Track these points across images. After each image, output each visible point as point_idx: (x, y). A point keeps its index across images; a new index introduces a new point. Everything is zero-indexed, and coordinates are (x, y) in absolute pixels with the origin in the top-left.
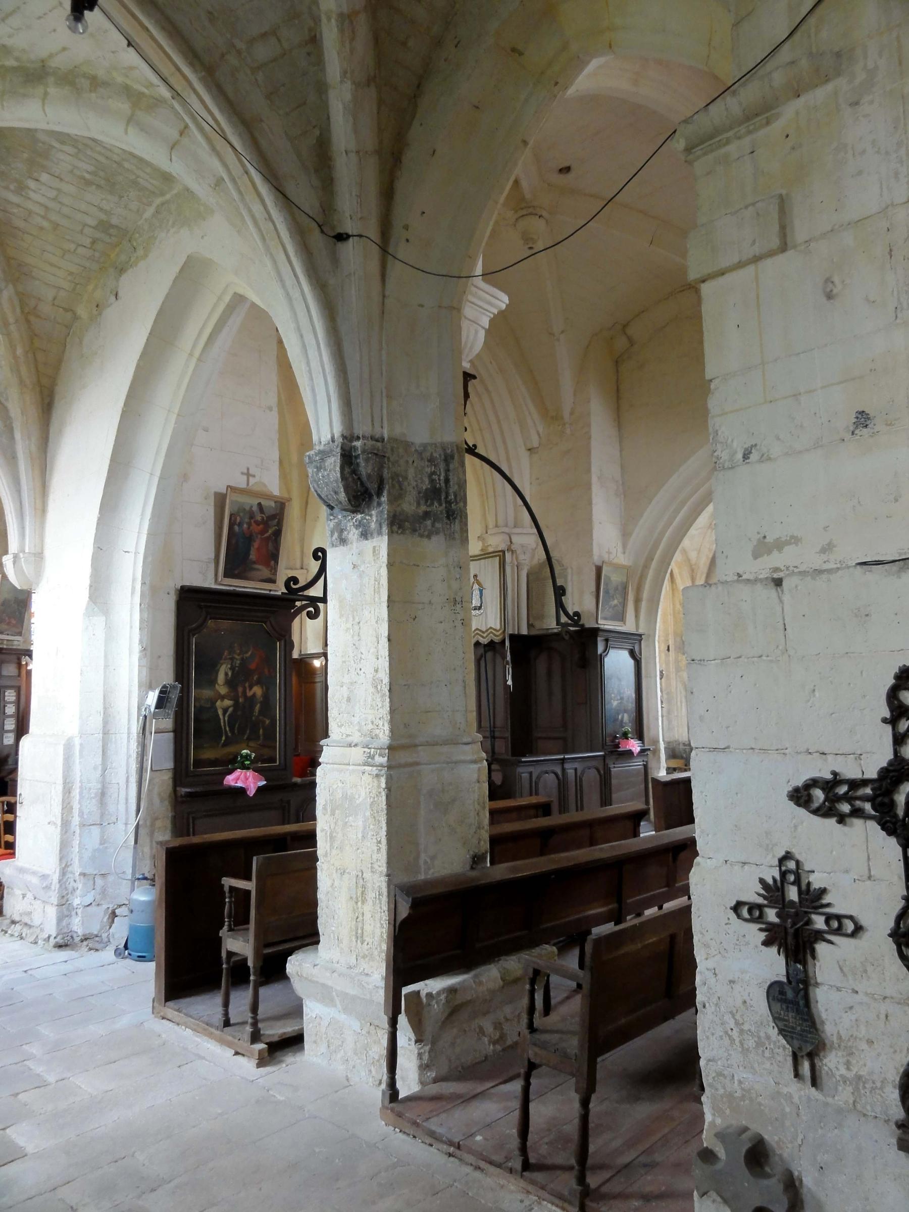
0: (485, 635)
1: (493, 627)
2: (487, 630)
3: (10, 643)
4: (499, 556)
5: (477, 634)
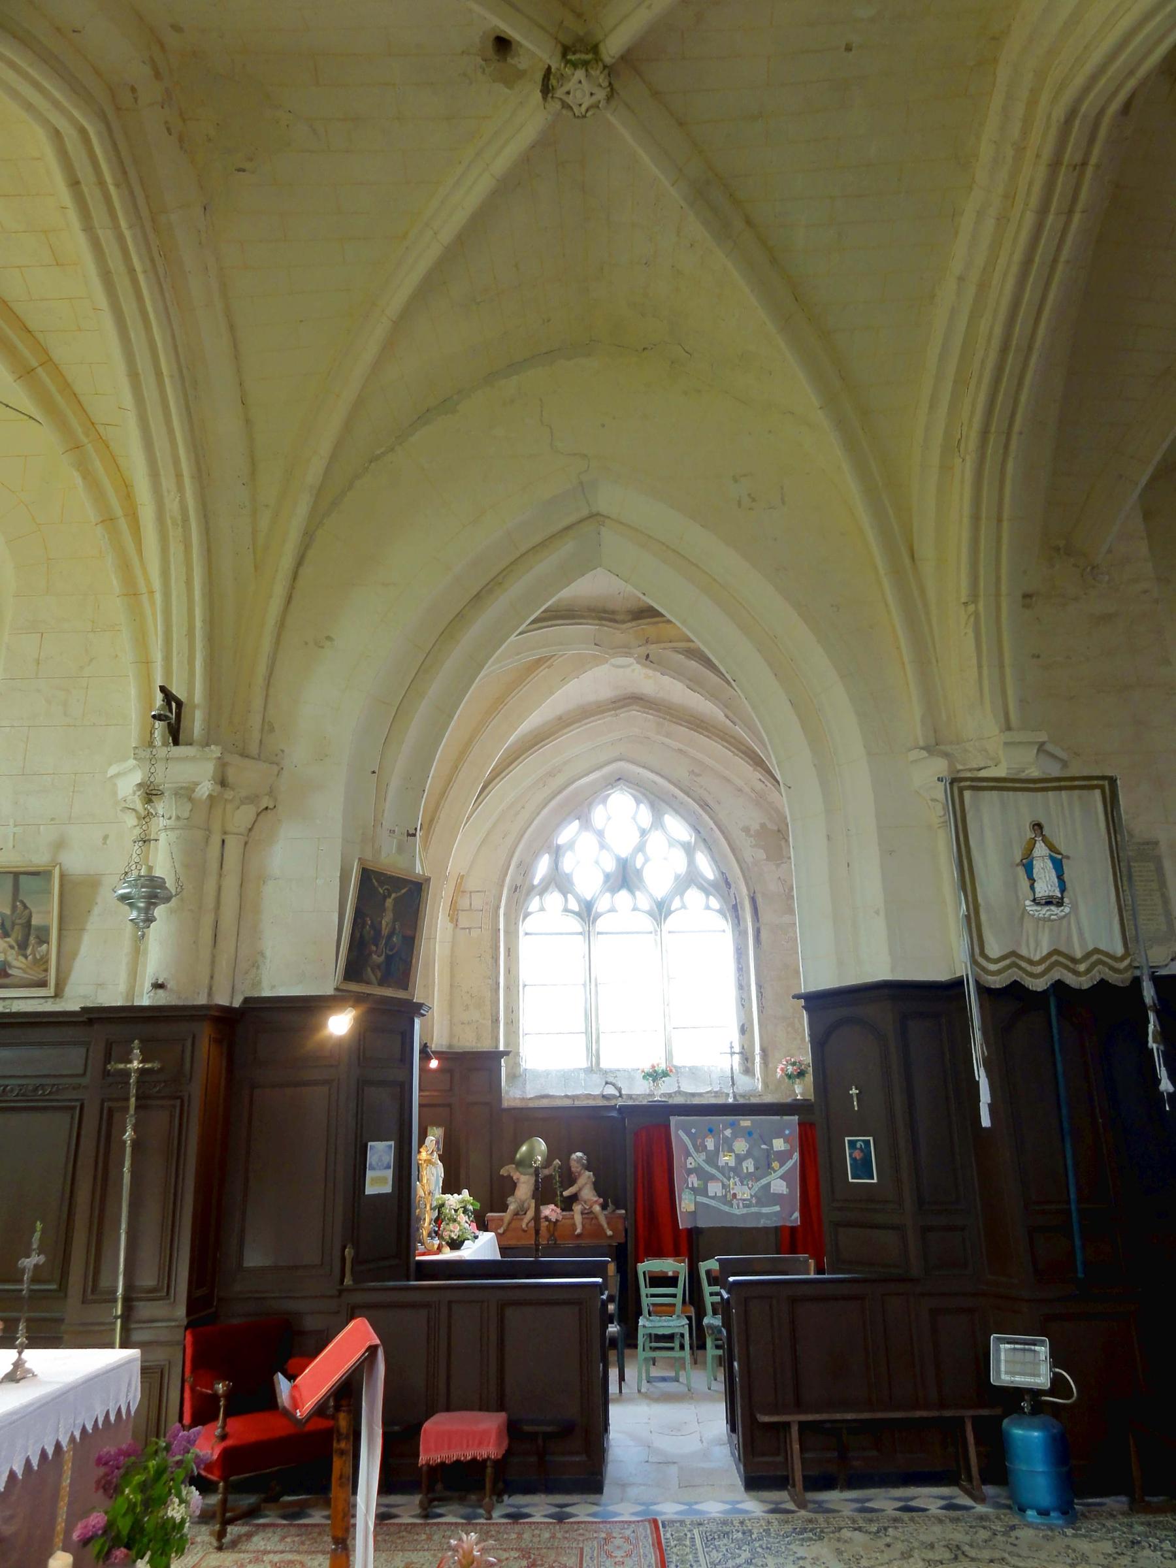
0: (1082, 968)
1: (1103, 947)
2: (1088, 955)
4: (1102, 788)
5: (1057, 963)
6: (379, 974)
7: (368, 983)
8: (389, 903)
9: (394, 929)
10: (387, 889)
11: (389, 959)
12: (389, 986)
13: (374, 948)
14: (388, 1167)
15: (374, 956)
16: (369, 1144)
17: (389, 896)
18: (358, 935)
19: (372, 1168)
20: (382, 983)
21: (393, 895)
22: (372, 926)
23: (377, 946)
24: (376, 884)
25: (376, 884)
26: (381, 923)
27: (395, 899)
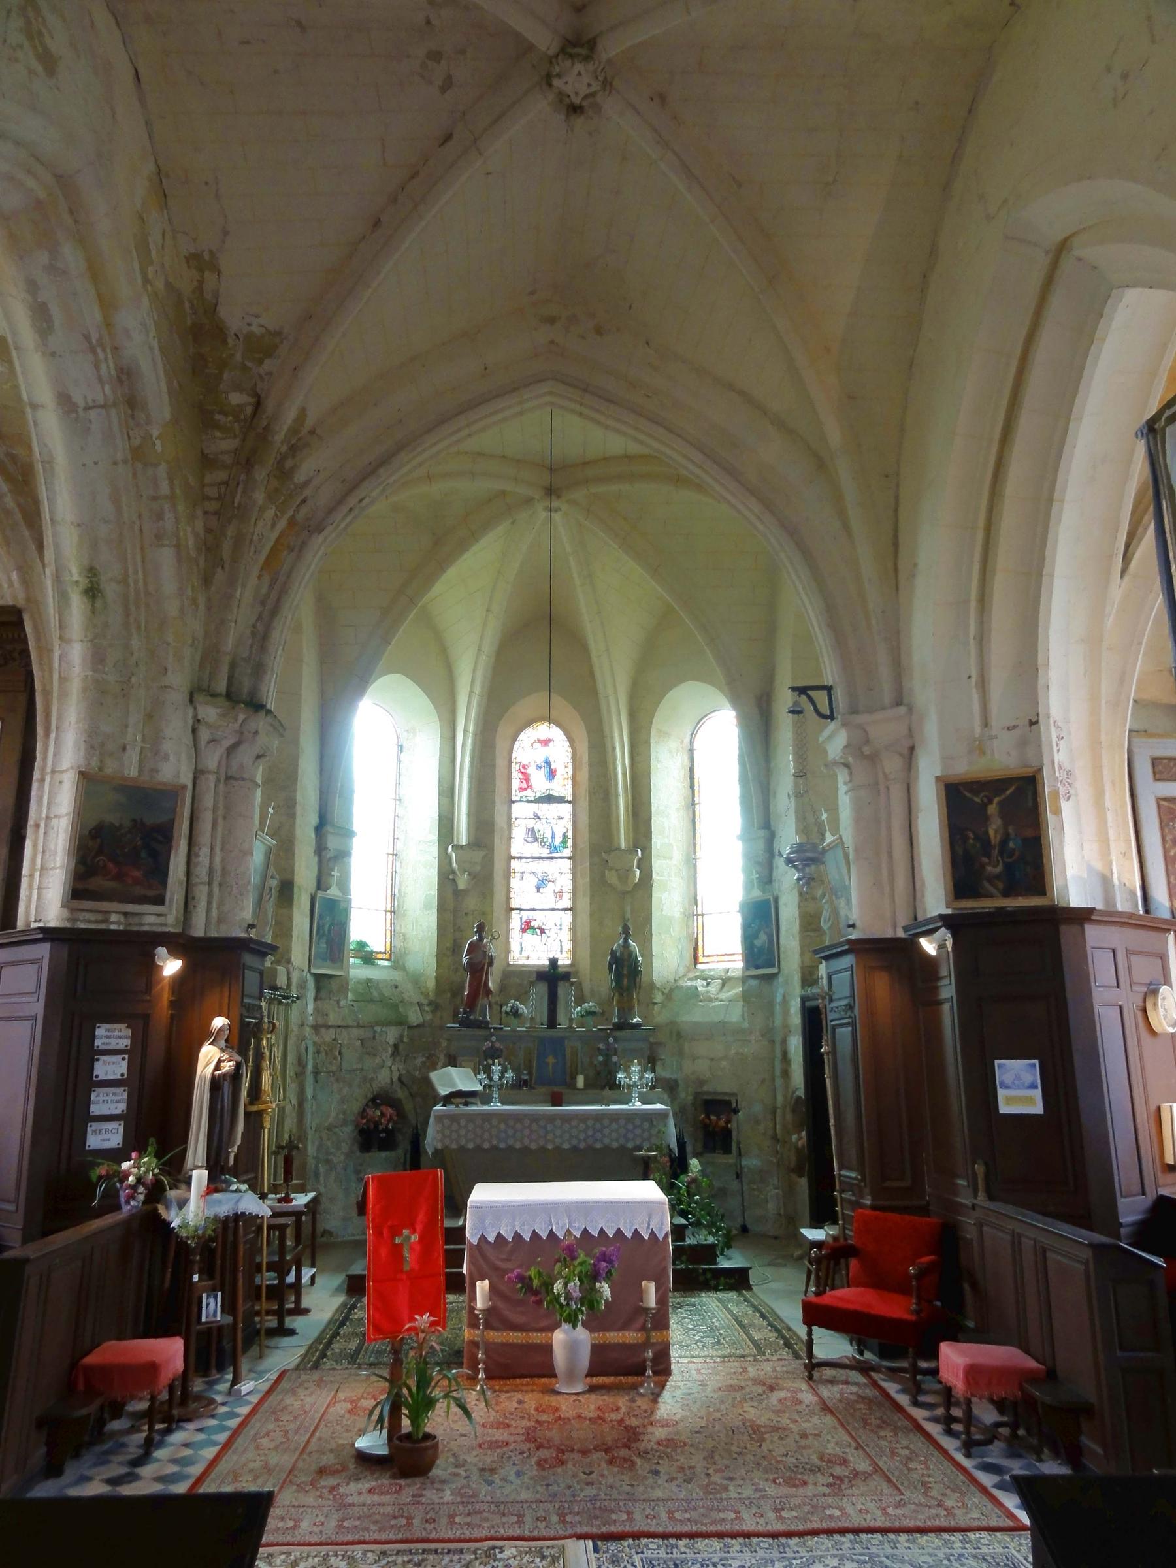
3: (136, 920)
6: (1001, 886)
7: (990, 896)
8: (992, 809)
9: (1008, 835)
10: (986, 796)
11: (1008, 867)
12: (1017, 895)
13: (985, 860)
14: (1033, 1086)
15: (989, 868)
16: (997, 1062)
17: (990, 801)
18: (960, 851)
19: (1005, 1086)
20: (1006, 894)
21: (996, 800)
22: (977, 838)
23: (989, 856)
24: (968, 795)
25: (968, 795)
26: (987, 833)
27: (999, 803)
